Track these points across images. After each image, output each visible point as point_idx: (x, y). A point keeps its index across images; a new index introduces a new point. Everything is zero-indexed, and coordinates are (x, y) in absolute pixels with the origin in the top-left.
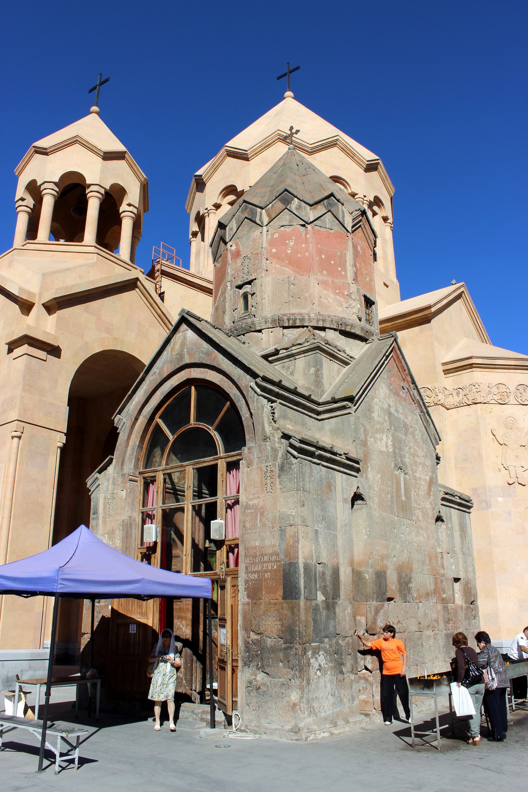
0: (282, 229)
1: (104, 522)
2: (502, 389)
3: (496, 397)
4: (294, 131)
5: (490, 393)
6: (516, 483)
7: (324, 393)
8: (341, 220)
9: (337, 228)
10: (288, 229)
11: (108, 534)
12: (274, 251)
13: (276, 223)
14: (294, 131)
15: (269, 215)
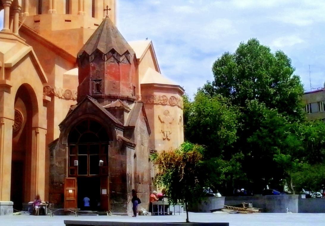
0: (111, 63)
1: (57, 159)
2: (165, 98)
3: (162, 102)
4: (108, 8)
5: (159, 100)
6: (166, 139)
7: (99, 102)
8: (129, 59)
9: (128, 62)
10: (113, 63)
11: (58, 162)
12: (108, 71)
13: (109, 60)
14: (108, 8)
15: (107, 57)
